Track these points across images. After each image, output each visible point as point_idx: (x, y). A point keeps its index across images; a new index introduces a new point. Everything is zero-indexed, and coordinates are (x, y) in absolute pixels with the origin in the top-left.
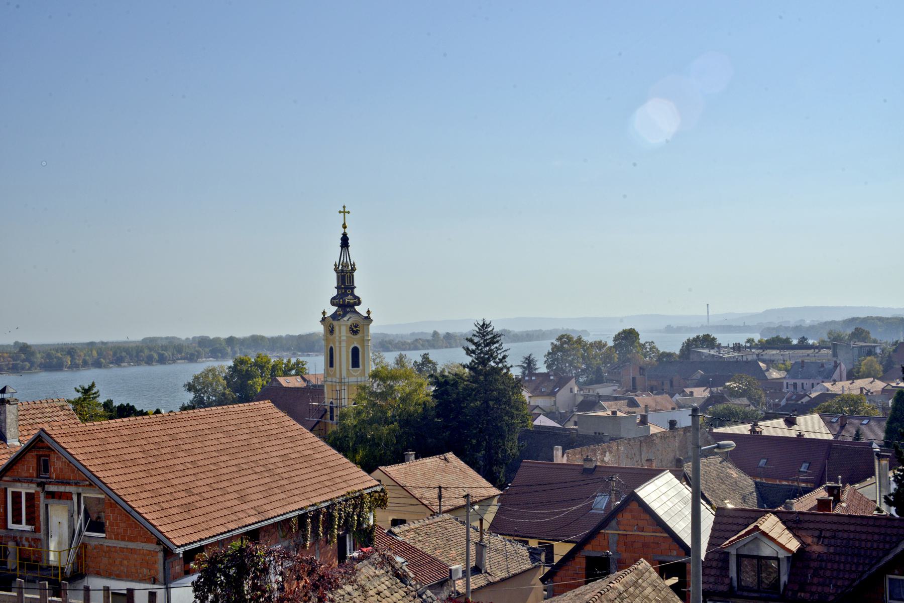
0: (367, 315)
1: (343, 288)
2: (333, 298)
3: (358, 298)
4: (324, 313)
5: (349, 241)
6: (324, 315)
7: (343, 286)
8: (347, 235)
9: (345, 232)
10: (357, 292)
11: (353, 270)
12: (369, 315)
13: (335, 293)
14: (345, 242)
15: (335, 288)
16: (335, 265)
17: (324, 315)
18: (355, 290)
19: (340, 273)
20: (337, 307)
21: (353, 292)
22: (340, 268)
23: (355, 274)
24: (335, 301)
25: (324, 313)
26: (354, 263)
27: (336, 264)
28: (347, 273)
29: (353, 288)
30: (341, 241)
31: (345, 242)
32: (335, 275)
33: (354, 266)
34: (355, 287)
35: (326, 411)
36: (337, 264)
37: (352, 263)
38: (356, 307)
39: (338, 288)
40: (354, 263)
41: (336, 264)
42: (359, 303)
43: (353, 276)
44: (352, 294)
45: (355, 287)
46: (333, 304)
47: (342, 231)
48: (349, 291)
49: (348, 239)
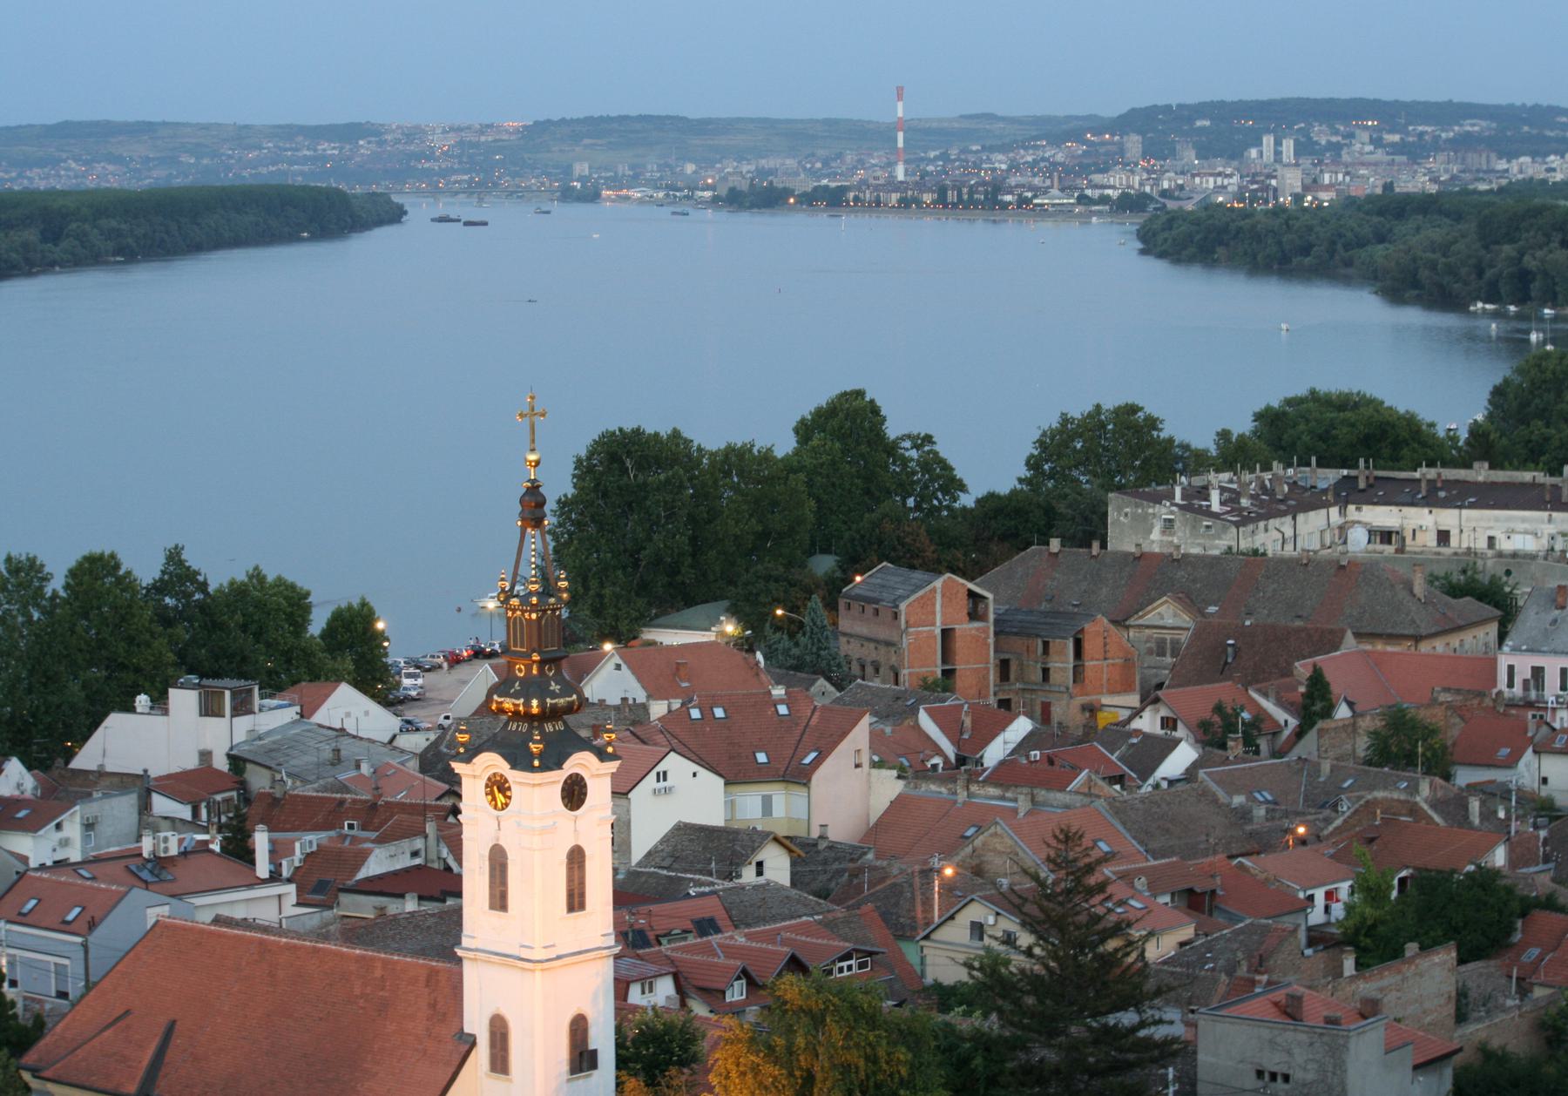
28: (545, 611)
30: (520, 508)
48: (550, 670)
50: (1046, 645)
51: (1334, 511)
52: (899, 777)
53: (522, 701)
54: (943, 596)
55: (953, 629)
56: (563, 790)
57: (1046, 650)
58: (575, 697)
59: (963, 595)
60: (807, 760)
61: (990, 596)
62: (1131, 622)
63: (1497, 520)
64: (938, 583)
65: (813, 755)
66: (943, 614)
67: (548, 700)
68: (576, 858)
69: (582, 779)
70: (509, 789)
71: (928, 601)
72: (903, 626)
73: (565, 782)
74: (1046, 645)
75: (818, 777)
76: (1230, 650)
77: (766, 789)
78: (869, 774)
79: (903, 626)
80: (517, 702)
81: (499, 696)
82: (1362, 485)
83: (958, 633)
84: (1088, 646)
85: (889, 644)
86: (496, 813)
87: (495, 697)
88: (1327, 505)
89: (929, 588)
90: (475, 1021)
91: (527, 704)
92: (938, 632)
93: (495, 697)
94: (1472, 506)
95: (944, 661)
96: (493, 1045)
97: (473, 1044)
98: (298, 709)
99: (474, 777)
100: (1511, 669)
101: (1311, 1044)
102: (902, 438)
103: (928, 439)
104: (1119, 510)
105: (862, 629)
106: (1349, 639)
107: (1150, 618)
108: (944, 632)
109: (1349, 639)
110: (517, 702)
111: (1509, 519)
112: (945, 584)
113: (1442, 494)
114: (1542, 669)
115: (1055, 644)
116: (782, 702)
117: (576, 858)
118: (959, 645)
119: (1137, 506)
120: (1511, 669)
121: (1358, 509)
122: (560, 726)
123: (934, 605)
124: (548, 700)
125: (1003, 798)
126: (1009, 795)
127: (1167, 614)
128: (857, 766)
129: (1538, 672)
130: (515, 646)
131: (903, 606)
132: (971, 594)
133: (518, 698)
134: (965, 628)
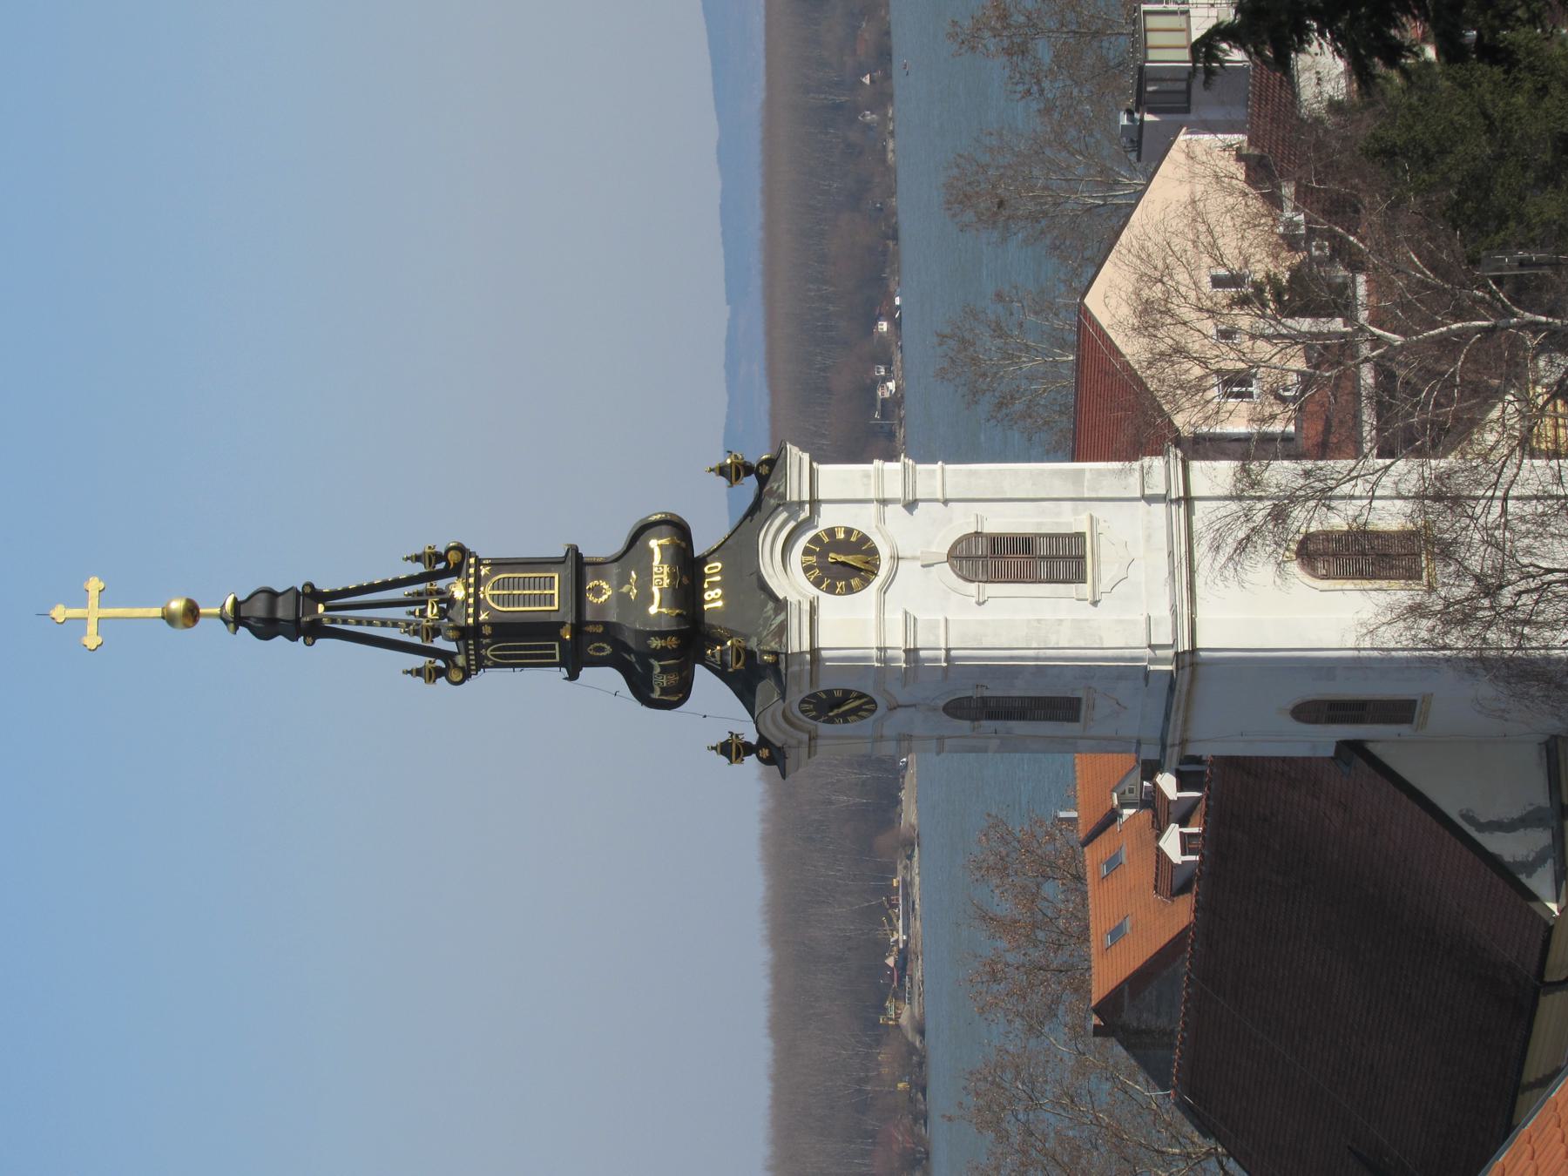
0: (751, 482)
2: (641, 690)
3: (643, 531)
4: (733, 750)
6: (747, 749)
9: (222, 617)
12: (748, 469)
13: (605, 681)
15: (573, 676)
16: (433, 675)
17: (747, 749)
18: (588, 552)
19: (478, 647)
24: (660, 681)
25: (733, 750)
26: (418, 558)
27: (419, 672)
33: (439, 557)
35: (1353, 750)
36: (420, 661)
37: (419, 568)
39: (574, 664)
40: (418, 558)
41: (419, 672)
42: (679, 530)
43: (498, 565)
46: (678, 694)
47: (211, 629)
48: (598, 591)
53: (656, 663)
56: (831, 590)
69: (816, 540)
70: (829, 692)
73: (817, 583)
80: (657, 670)
81: (652, 690)
86: (881, 711)
87: (656, 695)
91: (660, 654)
93: (656, 695)
97: (1353, 750)
99: (813, 738)
110: (657, 670)
122: (713, 568)
124: (653, 610)
130: (553, 656)
133: (651, 667)
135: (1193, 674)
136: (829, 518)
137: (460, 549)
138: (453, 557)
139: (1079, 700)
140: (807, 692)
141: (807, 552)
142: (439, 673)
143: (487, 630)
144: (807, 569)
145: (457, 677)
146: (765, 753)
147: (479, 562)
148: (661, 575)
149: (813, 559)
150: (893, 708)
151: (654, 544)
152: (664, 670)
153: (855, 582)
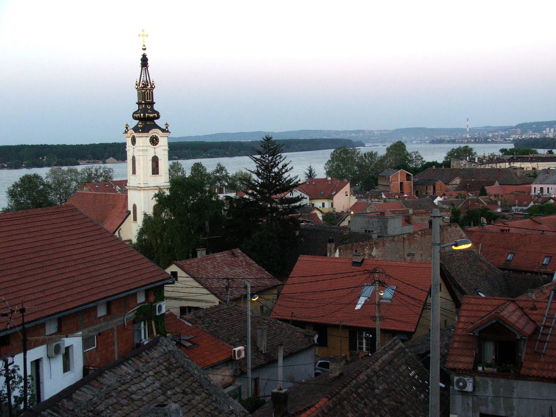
1: (143, 104)
5: (148, 62)
7: (143, 102)
8: (147, 56)
9: (144, 54)
10: (156, 107)
11: (152, 88)
13: (136, 108)
14: (144, 62)
15: (137, 103)
19: (141, 90)
20: (138, 121)
21: (152, 107)
22: (140, 86)
23: (155, 91)
24: (137, 115)
26: (153, 82)
27: (137, 82)
28: (147, 90)
29: (152, 103)
31: (144, 62)
32: (136, 91)
33: (153, 84)
34: (155, 103)
35: (129, 213)
36: (138, 82)
37: (151, 81)
38: (155, 121)
39: (139, 104)
40: (153, 82)
41: (137, 82)
42: (158, 117)
43: (152, 93)
44: (152, 109)
45: (155, 103)
46: (135, 118)
48: (149, 107)
49: (147, 60)
50: (427, 187)
51: (507, 164)
52: (356, 198)
54: (400, 174)
55: (403, 182)
56: (150, 139)
57: (427, 189)
58: (156, 114)
59: (405, 175)
60: (333, 194)
61: (412, 175)
62: (450, 183)
63: (547, 165)
64: (399, 171)
65: (335, 192)
66: (400, 179)
67: (147, 114)
68: (155, 160)
69: (157, 137)
71: (397, 175)
72: (391, 181)
73: (151, 137)
74: (427, 187)
75: (335, 198)
76: (468, 186)
77: (324, 201)
78: (350, 198)
79: (391, 181)
82: (515, 158)
83: (404, 183)
84: (437, 188)
85: (388, 186)
86: (133, 147)
87: (134, 115)
88: (505, 162)
89: (397, 172)
90: (130, 208)
92: (399, 183)
93: (134, 115)
94: (540, 162)
95: (401, 190)
96: (134, 213)
97: (130, 213)
98: (236, 193)
100: (535, 188)
101: (378, 222)
102: (412, 153)
103: (417, 152)
104: (453, 162)
105: (382, 183)
106: (497, 183)
107: (454, 182)
108: (400, 183)
109: (497, 183)
111: (549, 165)
112: (401, 171)
113: (534, 160)
114: (543, 188)
115: (429, 187)
116: (330, 181)
117: (155, 160)
118: (404, 186)
119: (458, 161)
120: (535, 188)
121: (513, 163)
123: (398, 177)
124: (147, 114)
125: (378, 202)
126: (380, 201)
127: (457, 181)
128: (347, 195)
129: (542, 189)
131: (390, 177)
132: (407, 174)
134: (406, 182)
135: (139, 190)
136: (160, 139)
137: (155, 87)
138: (153, 86)
139: (135, 174)
140: (135, 136)
141: (155, 136)
142: (137, 85)
143: (143, 91)
144: (153, 136)
145: (136, 87)
146: (127, 130)
147: (153, 90)
148: (151, 115)
149: (154, 136)
150: (134, 148)
151: (156, 114)
152: (138, 116)
153: (151, 143)
